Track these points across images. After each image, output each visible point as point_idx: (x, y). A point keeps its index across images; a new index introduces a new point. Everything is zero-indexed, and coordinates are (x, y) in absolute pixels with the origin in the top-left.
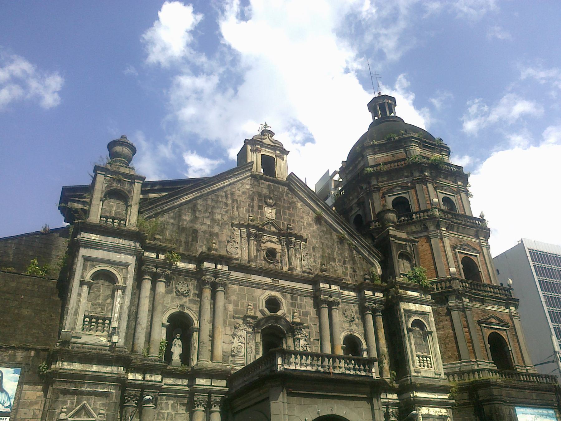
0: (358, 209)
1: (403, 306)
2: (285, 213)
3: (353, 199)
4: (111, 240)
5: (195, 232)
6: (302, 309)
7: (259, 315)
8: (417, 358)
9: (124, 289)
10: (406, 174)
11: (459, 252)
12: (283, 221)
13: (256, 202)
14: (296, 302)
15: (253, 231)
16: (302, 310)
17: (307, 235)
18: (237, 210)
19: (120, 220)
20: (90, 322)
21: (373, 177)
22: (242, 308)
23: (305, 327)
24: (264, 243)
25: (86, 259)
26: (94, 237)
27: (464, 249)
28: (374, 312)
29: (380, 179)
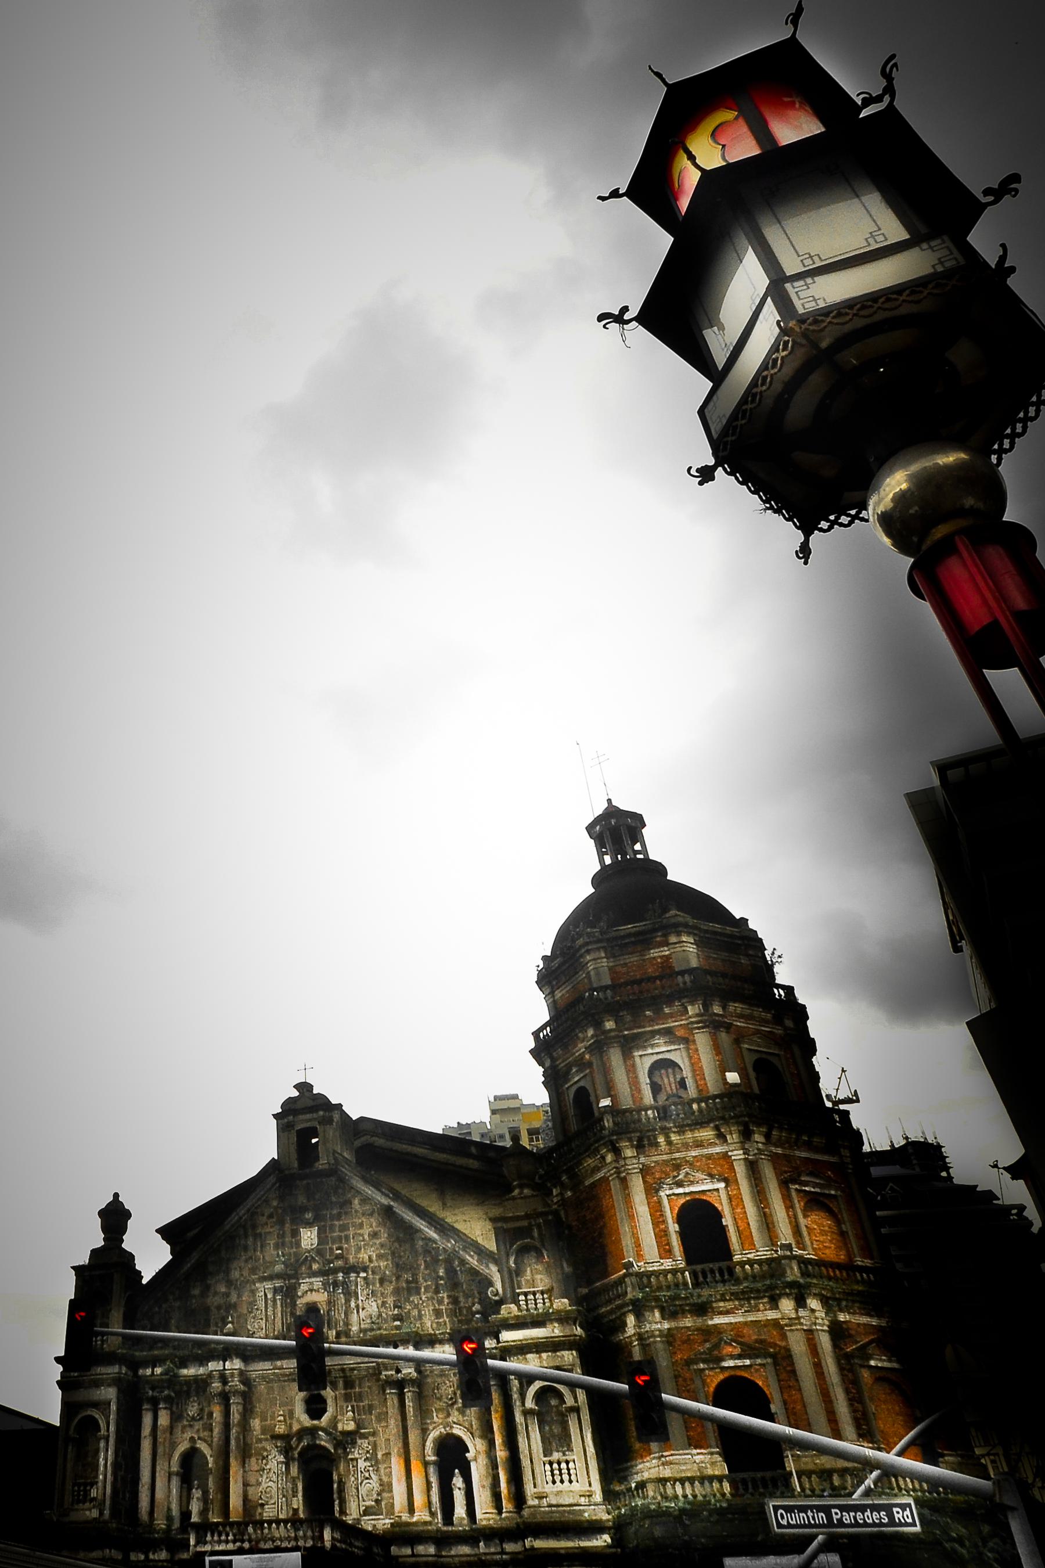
2: (332, 1228)
6: (362, 1402)
8: (548, 1467)
11: (667, 1196)
12: (330, 1245)
14: (353, 1391)
16: (362, 1404)
17: (370, 1257)
18: (262, 1251)
22: (273, 1422)
23: (364, 1436)
24: (300, 1297)
27: (680, 1184)
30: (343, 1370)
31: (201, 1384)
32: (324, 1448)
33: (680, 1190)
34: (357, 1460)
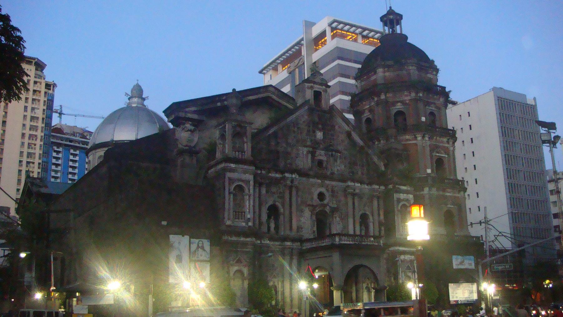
0: (369, 113)
1: (396, 196)
3: (366, 105)
4: (241, 166)
5: (278, 152)
7: (315, 204)
9: (249, 196)
10: (406, 94)
13: (311, 128)
15: (311, 149)
19: (242, 152)
20: (236, 214)
21: (382, 93)
25: (230, 179)
26: (233, 166)
28: (378, 198)
29: (387, 95)
30: (333, 186)
31: (277, 182)
32: (326, 212)
33: (437, 154)
34: (336, 217)
